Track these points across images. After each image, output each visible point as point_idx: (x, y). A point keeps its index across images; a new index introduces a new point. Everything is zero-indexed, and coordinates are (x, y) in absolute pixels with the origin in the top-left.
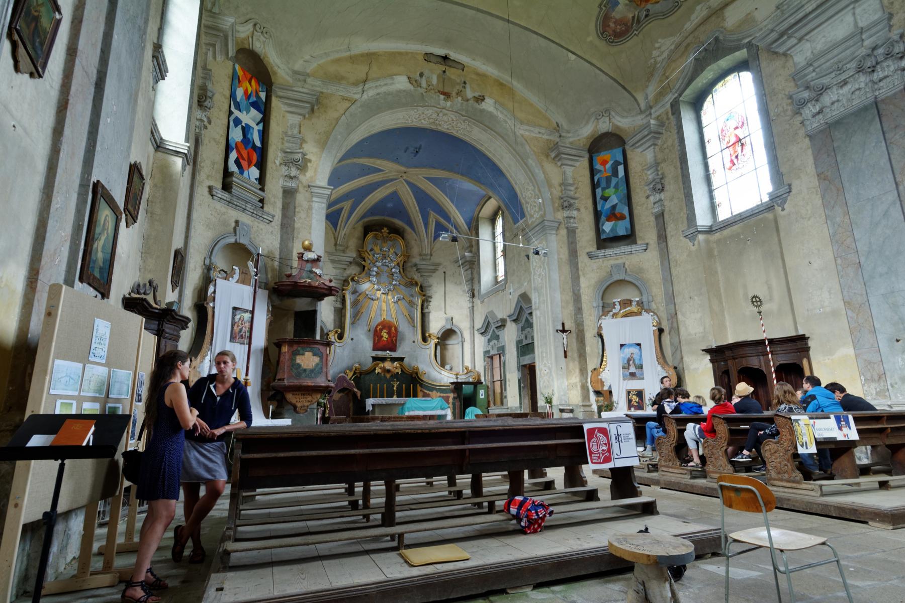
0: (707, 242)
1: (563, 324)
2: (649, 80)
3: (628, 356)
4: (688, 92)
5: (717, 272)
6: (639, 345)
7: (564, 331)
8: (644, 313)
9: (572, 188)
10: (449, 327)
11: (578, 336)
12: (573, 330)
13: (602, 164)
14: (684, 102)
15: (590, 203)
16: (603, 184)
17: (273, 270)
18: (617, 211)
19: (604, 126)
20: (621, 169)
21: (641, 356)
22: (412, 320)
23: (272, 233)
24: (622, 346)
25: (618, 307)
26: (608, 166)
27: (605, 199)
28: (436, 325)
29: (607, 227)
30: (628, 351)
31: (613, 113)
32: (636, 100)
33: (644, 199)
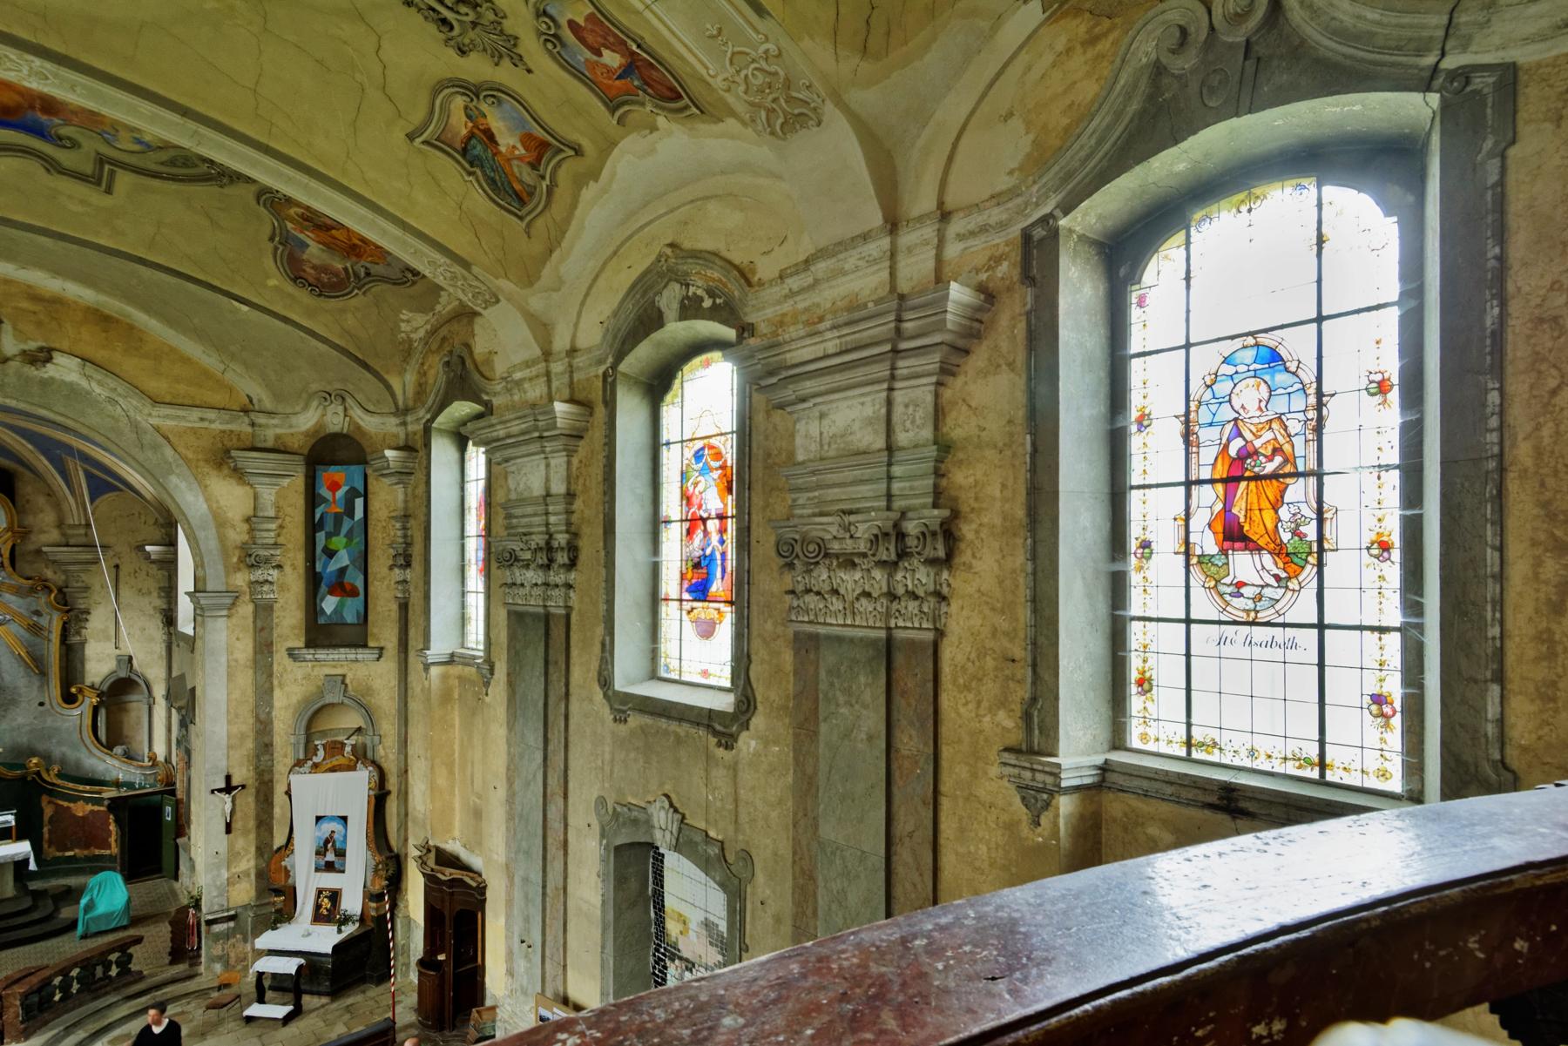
0: (445, 677)
1: (228, 778)
2: (405, 360)
4: (440, 419)
5: (453, 726)
6: (344, 819)
7: (228, 788)
8: (359, 765)
9: (273, 526)
10: (123, 674)
11: (258, 792)
13: (329, 488)
14: (440, 431)
15: (300, 558)
16: (329, 526)
18: (348, 579)
19: (335, 421)
20: (359, 502)
22: (37, 665)
24: (318, 819)
25: (321, 753)
26: (340, 493)
27: (331, 554)
28: (99, 665)
29: (329, 604)
30: (327, 828)
31: (349, 401)
32: (388, 387)
33: (385, 570)
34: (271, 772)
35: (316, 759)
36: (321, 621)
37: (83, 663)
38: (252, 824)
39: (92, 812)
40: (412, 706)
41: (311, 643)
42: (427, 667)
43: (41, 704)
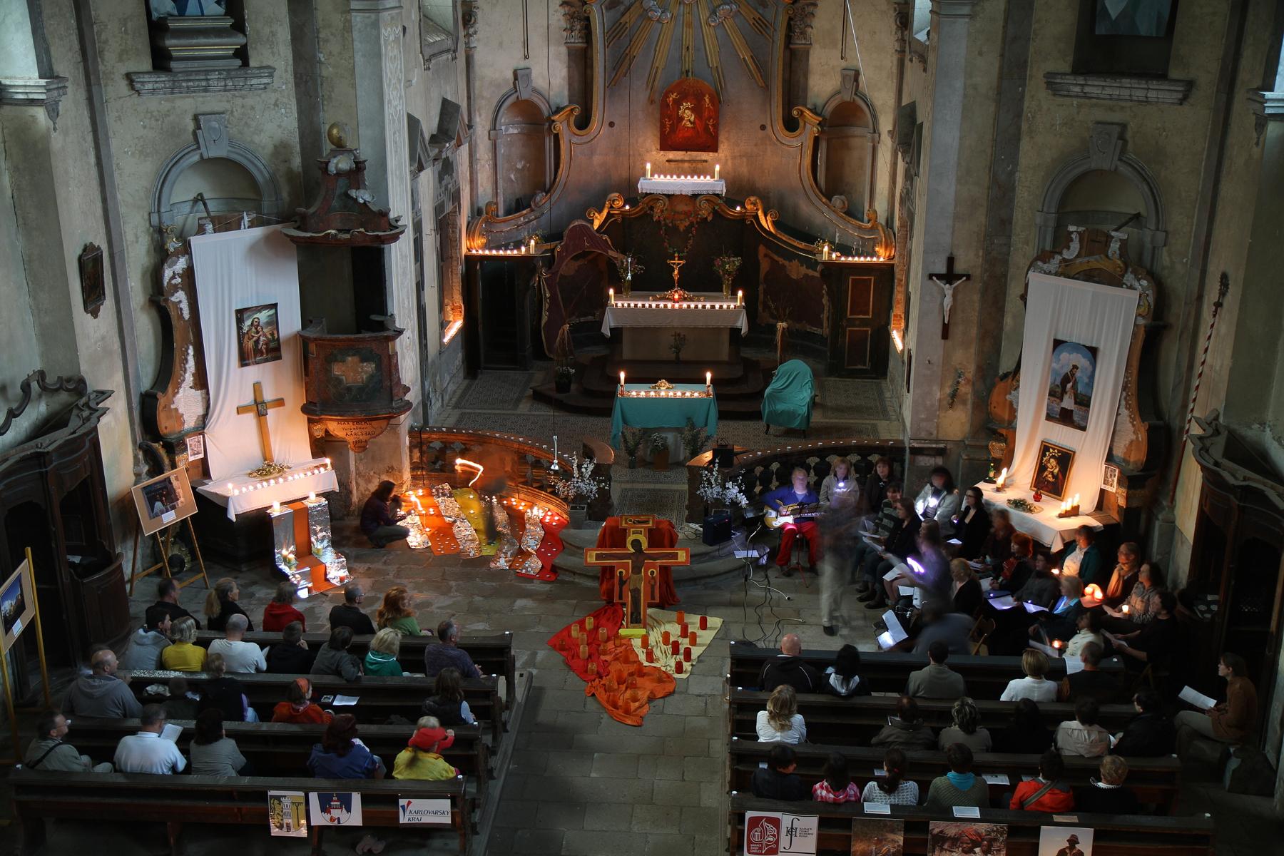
1: (951, 261)
3: (1067, 370)
6: (1093, 351)
7: (949, 277)
10: (847, 97)
12: (977, 273)
17: (291, 176)
21: (1092, 377)
23: (276, 105)
24: (1057, 343)
25: (1075, 246)
28: (823, 84)
30: (1069, 359)
34: (1006, 262)
35: (1067, 255)
36: (1101, 30)
37: (806, 79)
38: (974, 332)
39: (806, 275)
40: (1228, 189)
41: (1082, 68)
42: (1262, 121)
43: (763, 127)
